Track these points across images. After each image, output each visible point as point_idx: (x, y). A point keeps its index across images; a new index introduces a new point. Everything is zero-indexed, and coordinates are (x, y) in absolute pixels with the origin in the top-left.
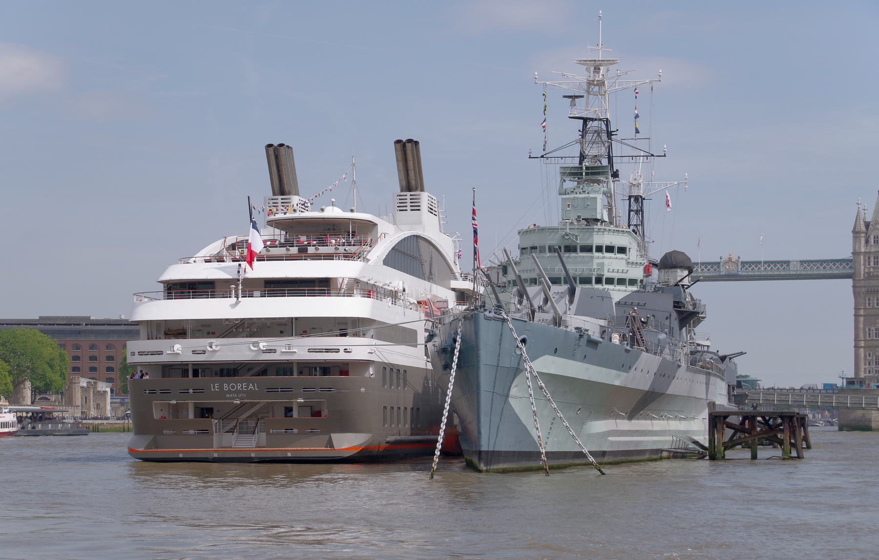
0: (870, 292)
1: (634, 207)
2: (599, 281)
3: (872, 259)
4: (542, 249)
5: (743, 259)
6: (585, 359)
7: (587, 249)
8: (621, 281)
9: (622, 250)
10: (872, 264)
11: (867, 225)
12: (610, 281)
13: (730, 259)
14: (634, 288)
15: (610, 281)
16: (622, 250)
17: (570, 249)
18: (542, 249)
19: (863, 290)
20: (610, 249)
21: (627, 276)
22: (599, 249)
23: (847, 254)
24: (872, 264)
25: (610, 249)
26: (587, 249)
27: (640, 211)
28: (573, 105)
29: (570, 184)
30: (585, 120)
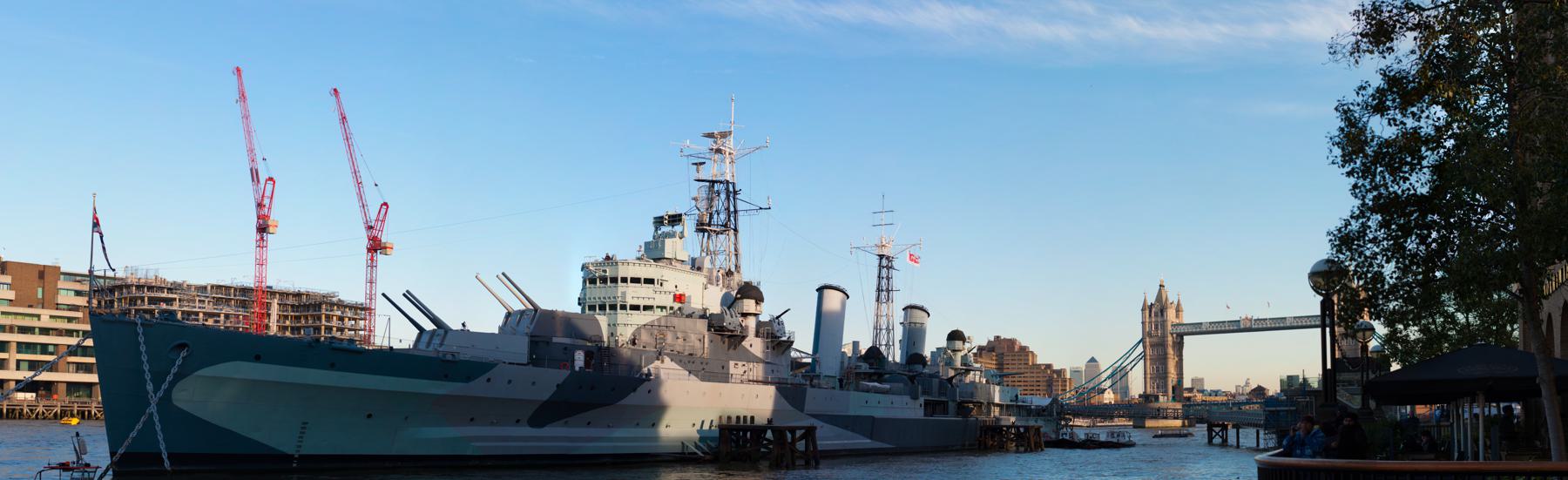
1: (884, 262)
2: (623, 307)
6: (333, 366)
8: (646, 308)
9: (650, 281)
12: (635, 308)
14: (664, 313)
15: (635, 308)
16: (650, 281)
20: (636, 280)
21: (655, 303)
22: (624, 280)
25: (636, 280)
26: (614, 280)
27: (889, 268)
29: (666, 229)
30: (713, 182)
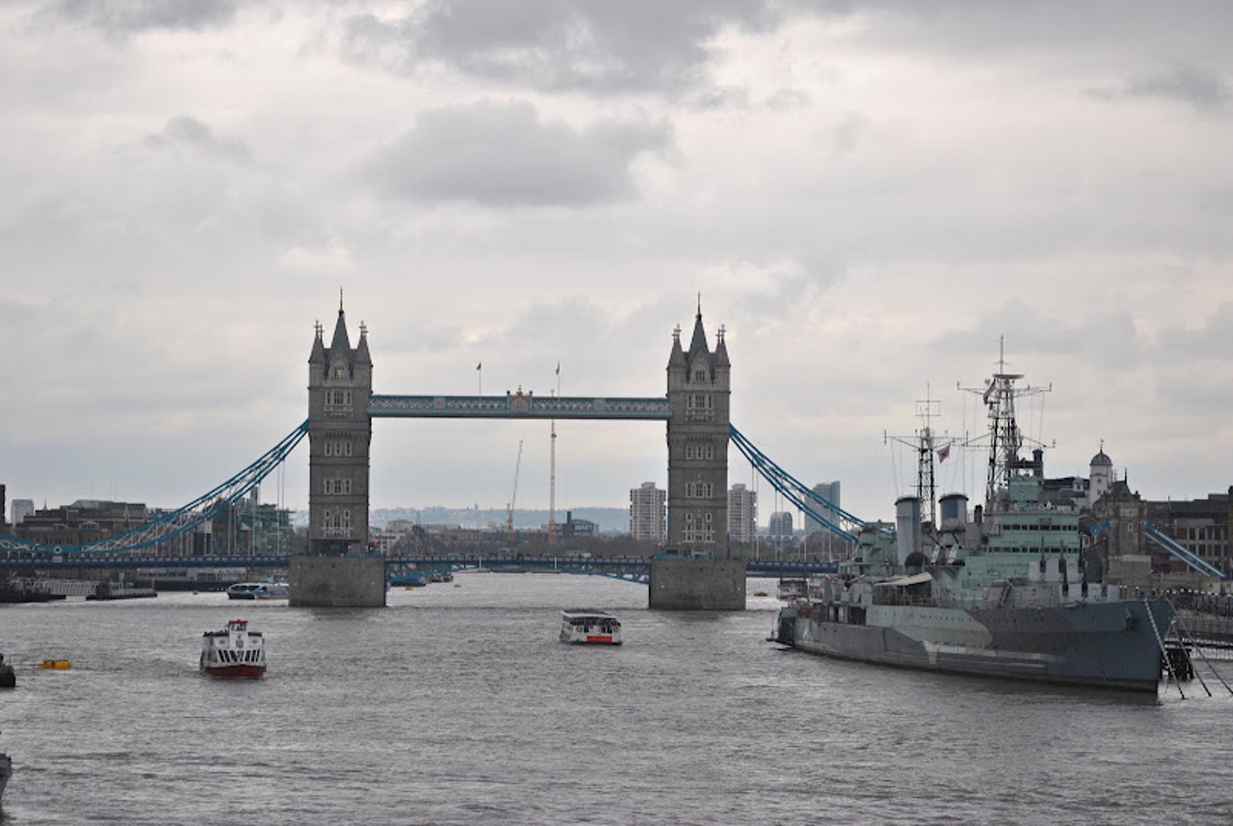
0: (691, 440)
3: (694, 399)
4: (1025, 527)
5: (534, 395)
7: (1056, 528)
10: (694, 405)
11: (686, 354)
13: (520, 394)
17: (1045, 528)
18: (1025, 527)
19: (684, 437)
22: (1064, 528)
23: (662, 393)
24: (694, 405)
26: (1056, 528)
28: (991, 408)
